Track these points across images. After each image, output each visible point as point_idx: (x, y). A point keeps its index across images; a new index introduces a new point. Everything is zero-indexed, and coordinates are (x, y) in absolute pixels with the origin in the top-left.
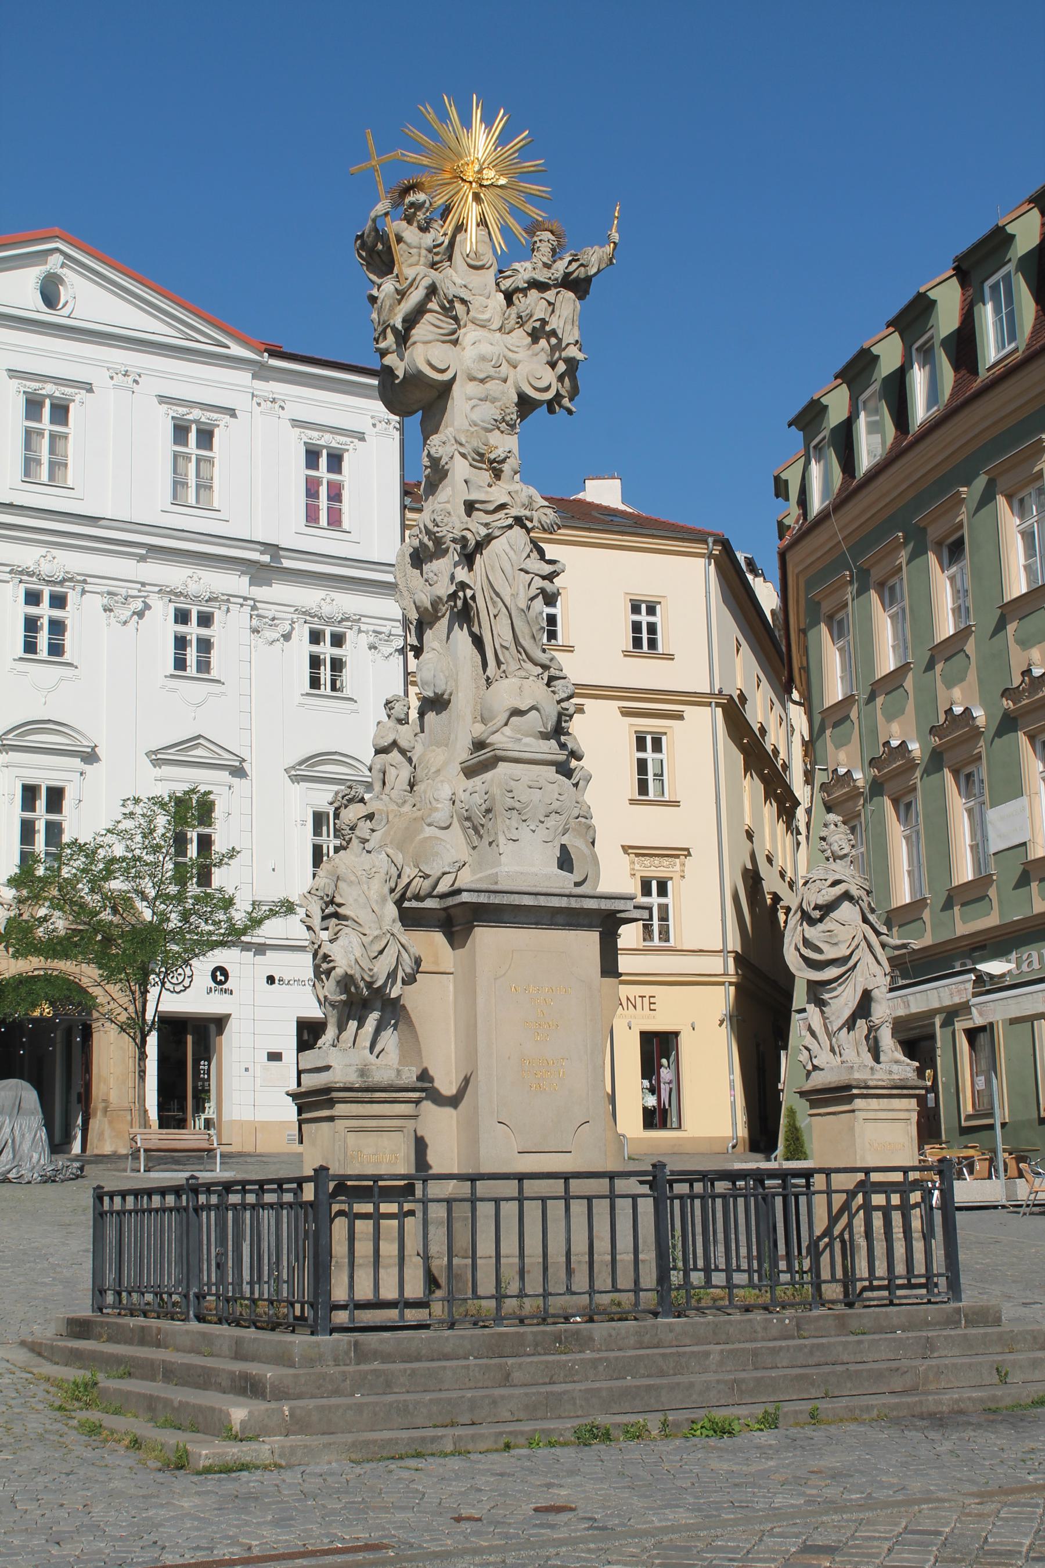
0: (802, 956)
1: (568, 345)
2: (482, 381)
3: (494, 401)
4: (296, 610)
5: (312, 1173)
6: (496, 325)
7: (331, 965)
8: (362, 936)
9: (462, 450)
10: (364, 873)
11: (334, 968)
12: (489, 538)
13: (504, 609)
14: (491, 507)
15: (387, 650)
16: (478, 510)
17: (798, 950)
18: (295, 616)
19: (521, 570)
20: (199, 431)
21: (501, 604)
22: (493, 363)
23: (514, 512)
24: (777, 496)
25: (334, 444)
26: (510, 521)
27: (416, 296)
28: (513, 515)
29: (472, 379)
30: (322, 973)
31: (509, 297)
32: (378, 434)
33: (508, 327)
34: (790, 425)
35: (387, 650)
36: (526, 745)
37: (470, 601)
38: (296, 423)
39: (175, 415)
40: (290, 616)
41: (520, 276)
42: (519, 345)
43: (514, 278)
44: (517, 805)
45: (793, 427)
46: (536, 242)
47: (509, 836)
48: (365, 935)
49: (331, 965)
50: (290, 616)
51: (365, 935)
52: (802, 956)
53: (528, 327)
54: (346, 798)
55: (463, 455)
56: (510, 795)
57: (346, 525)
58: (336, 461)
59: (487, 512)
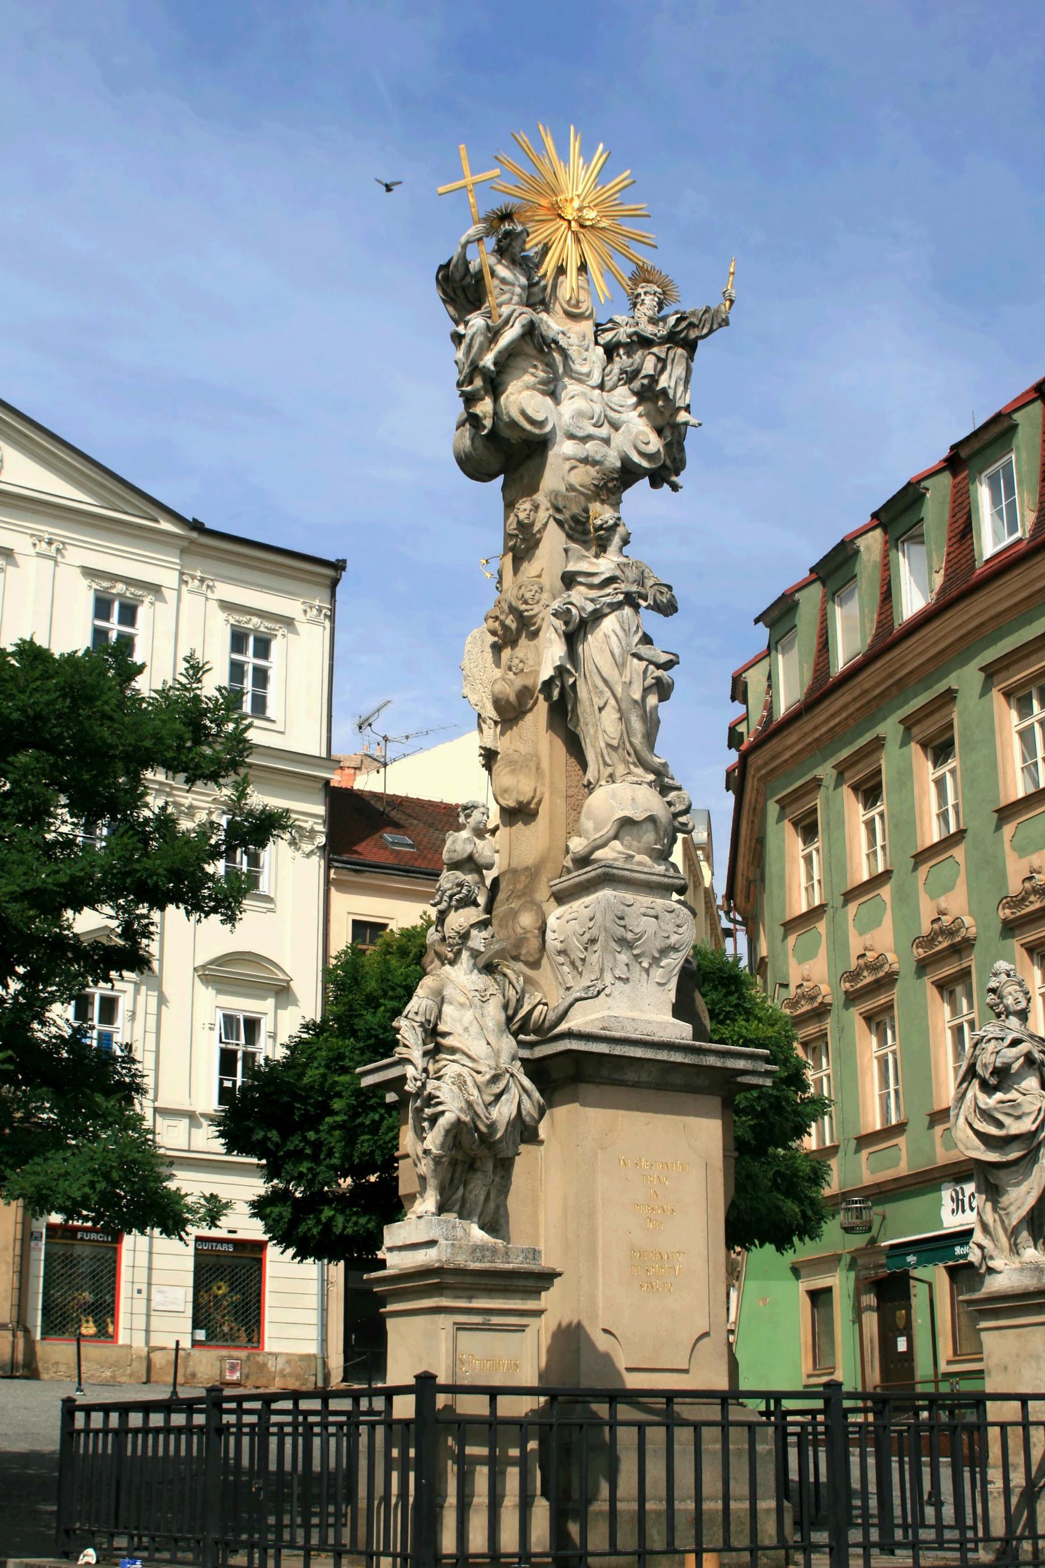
0: (977, 1133)
1: (679, 409)
2: (585, 439)
3: (595, 463)
4: (215, 799)
5: (412, 1381)
6: (596, 379)
7: (440, 1108)
8: (475, 1074)
9: (558, 516)
10: (477, 994)
11: (443, 1113)
12: (597, 616)
13: (612, 702)
14: (596, 580)
15: (307, 847)
16: (581, 584)
17: (970, 1125)
18: (212, 806)
19: (635, 655)
20: (122, 606)
21: (608, 694)
22: (594, 421)
23: (623, 587)
24: (733, 698)
25: (262, 629)
26: (621, 597)
27: (509, 335)
28: (624, 590)
29: (571, 437)
30: (425, 1120)
31: (610, 351)
32: (310, 621)
33: (608, 385)
34: (757, 621)
35: (307, 847)
36: (640, 864)
37: (568, 689)
38: (226, 606)
39: (98, 588)
40: (207, 805)
41: (622, 330)
42: (623, 403)
43: (614, 332)
44: (630, 936)
45: (761, 624)
46: (640, 294)
47: (618, 973)
48: (479, 1072)
49: (440, 1108)
50: (207, 805)
51: (479, 1072)
52: (977, 1133)
53: (636, 385)
54: (457, 897)
55: (560, 523)
56: (622, 923)
57: (269, 713)
58: (263, 648)
59: (591, 586)
